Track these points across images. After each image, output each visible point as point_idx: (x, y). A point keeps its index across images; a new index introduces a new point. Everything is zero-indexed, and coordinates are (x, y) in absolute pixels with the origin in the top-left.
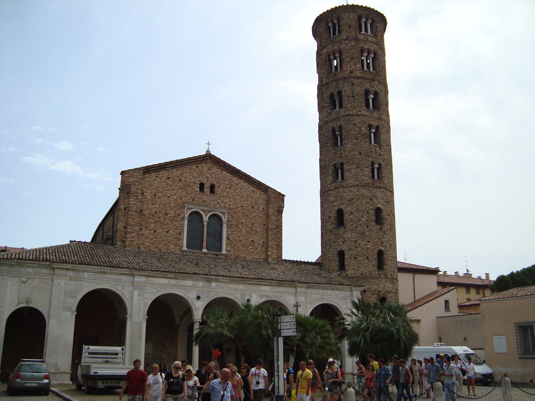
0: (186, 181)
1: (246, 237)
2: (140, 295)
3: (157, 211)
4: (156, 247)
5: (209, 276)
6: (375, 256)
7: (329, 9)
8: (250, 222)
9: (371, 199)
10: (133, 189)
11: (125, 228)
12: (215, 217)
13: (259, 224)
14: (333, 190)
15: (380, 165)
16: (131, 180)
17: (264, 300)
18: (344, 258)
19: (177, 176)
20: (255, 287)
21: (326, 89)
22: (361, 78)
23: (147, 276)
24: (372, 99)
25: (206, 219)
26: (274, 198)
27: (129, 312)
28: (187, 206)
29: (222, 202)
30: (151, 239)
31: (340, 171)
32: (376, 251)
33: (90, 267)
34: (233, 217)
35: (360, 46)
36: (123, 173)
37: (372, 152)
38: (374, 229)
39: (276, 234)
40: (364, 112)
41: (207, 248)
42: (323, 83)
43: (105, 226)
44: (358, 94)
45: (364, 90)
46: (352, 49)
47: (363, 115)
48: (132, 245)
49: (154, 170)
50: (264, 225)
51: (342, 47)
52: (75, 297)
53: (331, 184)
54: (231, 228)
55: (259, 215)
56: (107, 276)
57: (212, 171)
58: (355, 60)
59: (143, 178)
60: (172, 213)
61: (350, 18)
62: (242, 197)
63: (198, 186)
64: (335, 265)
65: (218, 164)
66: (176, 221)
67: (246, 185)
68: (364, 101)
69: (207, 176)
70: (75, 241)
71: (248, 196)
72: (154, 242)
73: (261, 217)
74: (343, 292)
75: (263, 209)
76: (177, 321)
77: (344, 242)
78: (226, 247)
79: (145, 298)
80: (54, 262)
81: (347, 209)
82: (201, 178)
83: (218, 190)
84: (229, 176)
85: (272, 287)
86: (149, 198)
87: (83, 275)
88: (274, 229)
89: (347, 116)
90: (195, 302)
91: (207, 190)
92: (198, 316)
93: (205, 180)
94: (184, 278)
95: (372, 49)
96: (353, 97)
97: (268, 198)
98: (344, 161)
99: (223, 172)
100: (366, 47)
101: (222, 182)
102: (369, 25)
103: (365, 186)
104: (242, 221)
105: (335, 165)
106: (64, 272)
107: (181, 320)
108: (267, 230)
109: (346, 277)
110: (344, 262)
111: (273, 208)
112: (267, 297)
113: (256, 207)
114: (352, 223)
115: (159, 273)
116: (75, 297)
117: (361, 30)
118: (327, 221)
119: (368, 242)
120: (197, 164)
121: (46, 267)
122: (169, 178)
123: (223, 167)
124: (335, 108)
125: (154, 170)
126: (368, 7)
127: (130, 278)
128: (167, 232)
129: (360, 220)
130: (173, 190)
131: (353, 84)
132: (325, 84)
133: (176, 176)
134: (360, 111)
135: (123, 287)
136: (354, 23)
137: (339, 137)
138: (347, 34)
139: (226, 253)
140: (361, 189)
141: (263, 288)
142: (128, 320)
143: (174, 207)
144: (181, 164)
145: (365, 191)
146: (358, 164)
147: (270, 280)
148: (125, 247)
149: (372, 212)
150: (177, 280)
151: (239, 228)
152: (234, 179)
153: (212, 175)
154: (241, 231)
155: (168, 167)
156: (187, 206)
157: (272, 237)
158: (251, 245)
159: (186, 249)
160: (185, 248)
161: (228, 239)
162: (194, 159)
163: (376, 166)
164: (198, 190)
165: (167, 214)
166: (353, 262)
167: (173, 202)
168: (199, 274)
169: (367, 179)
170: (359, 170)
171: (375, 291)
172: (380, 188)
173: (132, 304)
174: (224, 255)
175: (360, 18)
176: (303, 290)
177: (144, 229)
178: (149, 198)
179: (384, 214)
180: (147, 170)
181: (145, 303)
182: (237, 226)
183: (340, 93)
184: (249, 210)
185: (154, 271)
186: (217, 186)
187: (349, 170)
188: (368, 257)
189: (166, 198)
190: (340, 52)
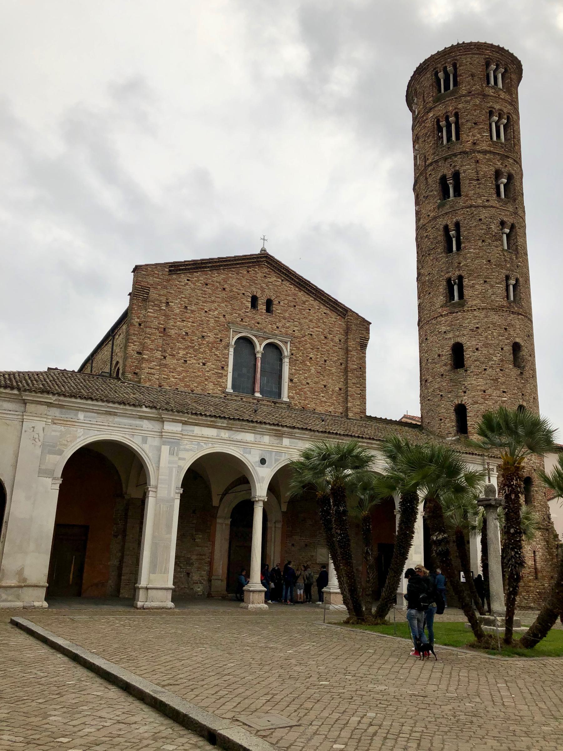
0: (231, 291)
1: (316, 380)
2: (172, 453)
3: (190, 331)
4: (186, 386)
5: (280, 428)
7: (441, 49)
9: (506, 329)
10: (153, 294)
11: (139, 353)
12: (273, 347)
14: (447, 315)
15: (517, 280)
16: (151, 280)
18: (465, 416)
19: (219, 283)
21: (433, 170)
22: (490, 152)
23: (185, 423)
24: (505, 186)
27: (153, 482)
29: (283, 327)
30: (179, 373)
31: (456, 287)
33: (90, 402)
34: (298, 349)
35: (489, 105)
36: (137, 269)
37: (506, 261)
40: (494, 201)
41: (261, 393)
42: (428, 162)
43: (94, 362)
44: (485, 176)
45: (494, 170)
46: (475, 110)
47: (494, 207)
48: (150, 380)
49: (186, 269)
50: (341, 364)
51: (460, 106)
52: (60, 453)
53: (442, 307)
54: (295, 365)
55: (336, 348)
56: (117, 419)
58: (481, 126)
59: (168, 281)
60: (211, 337)
61: (470, 65)
62: (311, 321)
63: (250, 300)
64: (450, 424)
66: (217, 349)
67: (316, 304)
68: (494, 187)
69: (261, 287)
70: (56, 369)
71: (318, 320)
72: (184, 377)
75: (340, 341)
76: (215, 503)
77: (465, 392)
78: (288, 394)
79: (180, 459)
80: (25, 390)
81: (469, 343)
82: (254, 289)
84: (293, 289)
87: (76, 415)
88: (355, 369)
89: (467, 208)
90: (258, 469)
91: (262, 307)
92: (261, 491)
94: (243, 430)
95: (505, 110)
96: (478, 180)
97: (347, 325)
98: (464, 274)
100: (497, 107)
102: (500, 76)
103: (498, 309)
104: (311, 356)
105: (449, 281)
106: (43, 408)
107: (221, 500)
108: (346, 371)
109: (469, 444)
110: (466, 421)
111: (354, 340)
114: (477, 363)
115: (204, 418)
116: (60, 453)
117: (488, 82)
118: (436, 361)
119: (504, 392)
120: (249, 267)
121: (11, 399)
122: (207, 285)
123: (286, 274)
124: (449, 197)
125: (186, 269)
126: (501, 46)
127: (156, 426)
128: (204, 364)
130: (213, 302)
131: (478, 161)
132: (431, 164)
133: (217, 282)
134: (488, 201)
135: (145, 440)
136: (479, 71)
137: (454, 240)
138: (469, 87)
139: (288, 400)
140: (491, 313)
142: (151, 494)
143: (214, 328)
144: (225, 265)
145: (496, 317)
146: (486, 277)
147: (370, 439)
148: (139, 382)
149: (508, 348)
150: (231, 432)
151: (306, 365)
152: (300, 294)
153: (269, 286)
154: (309, 370)
155: (206, 267)
157: (354, 381)
158: (322, 392)
159: (232, 391)
160: (229, 390)
161: (291, 380)
162: (244, 259)
163: (513, 282)
164: (249, 305)
165: (203, 337)
167: (212, 321)
168: (265, 423)
169: (500, 300)
170: (487, 286)
172: (519, 314)
173: (158, 467)
174: (286, 403)
175: (488, 65)
177: (168, 357)
178: (177, 311)
179: (524, 352)
180: (176, 268)
181: (179, 466)
182: (303, 362)
183: (456, 176)
185: (196, 414)
186: (275, 302)
187: (473, 286)
189: (203, 313)
190: (456, 115)
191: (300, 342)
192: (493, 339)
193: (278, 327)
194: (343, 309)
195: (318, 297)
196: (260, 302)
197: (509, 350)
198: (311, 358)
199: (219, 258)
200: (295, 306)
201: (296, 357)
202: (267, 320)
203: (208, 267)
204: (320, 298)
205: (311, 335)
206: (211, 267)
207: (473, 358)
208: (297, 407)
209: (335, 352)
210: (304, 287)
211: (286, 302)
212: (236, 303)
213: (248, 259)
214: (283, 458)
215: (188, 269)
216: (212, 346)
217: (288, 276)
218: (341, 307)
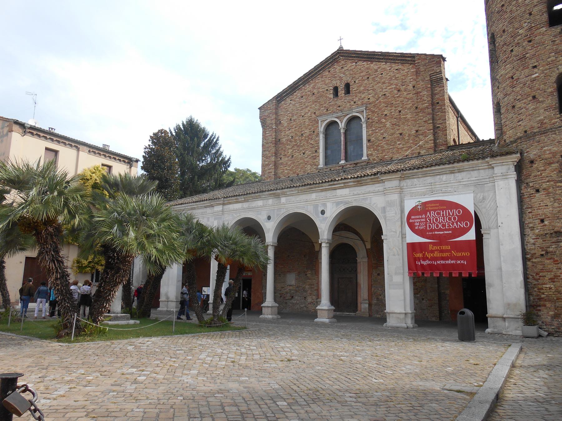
1: (392, 131)
3: (293, 134)
4: (294, 173)
5: (275, 192)
6: (550, 90)
8: (395, 110)
13: (410, 109)
17: (342, 208)
20: (329, 194)
25: (342, 125)
26: (425, 65)
28: (320, 119)
29: (359, 99)
32: (554, 78)
38: (546, 37)
39: (429, 114)
48: (270, 177)
49: (287, 94)
54: (371, 127)
57: (346, 68)
62: (384, 83)
65: (351, 57)
66: (311, 139)
67: (387, 66)
71: (391, 79)
72: (293, 167)
73: (411, 98)
74: (475, 174)
82: (334, 82)
83: (353, 88)
85: (352, 189)
86: (286, 124)
93: (339, 82)
99: (360, 63)
101: (357, 76)
104: (385, 113)
111: (423, 81)
112: (346, 203)
113: (402, 88)
119: (535, 67)
122: (302, 97)
125: (287, 94)
128: (304, 153)
129: (514, 36)
130: (307, 107)
139: (366, 158)
141: (339, 192)
143: (309, 125)
144: (311, 77)
151: (382, 123)
152: (372, 65)
154: (385, 126)
155: (299, 86)
156: (320, 119)
158: (399, 140)
161: (369, 141)
162: (322, 65)
164: (332, 96)
166: (511, 115)
167: (307, 120)
171: (554, 156)
176: (395, 183)
178: (286, 124)
182: (379, 122)
184: (393, 97)
188: (534, 97)
189: (301, 118)
191: (374, 106)
192: (518, 8)
193: (355, 102)
194: (411, 57)
195: (387, 59)
196: (339, 90)
197: (540, 11)
198: (386, 115)
199: (304, 75)
200: (368, 78)
201: (372, 119)
202: (346, 101)
203: (301, 84)
204: (389, 59)
205: (385, 94)
206: (303, 83)
207: (502, 43)
208: (375, 162)
209: (408, 99)
210: (374, 58)
211: (360, 78)
212: (321, 100)
213: (325, 62)
214: (282, 212)
215: (289, 93)
216: (309, 137)
217: (359, 57)
218: (409, 57)
